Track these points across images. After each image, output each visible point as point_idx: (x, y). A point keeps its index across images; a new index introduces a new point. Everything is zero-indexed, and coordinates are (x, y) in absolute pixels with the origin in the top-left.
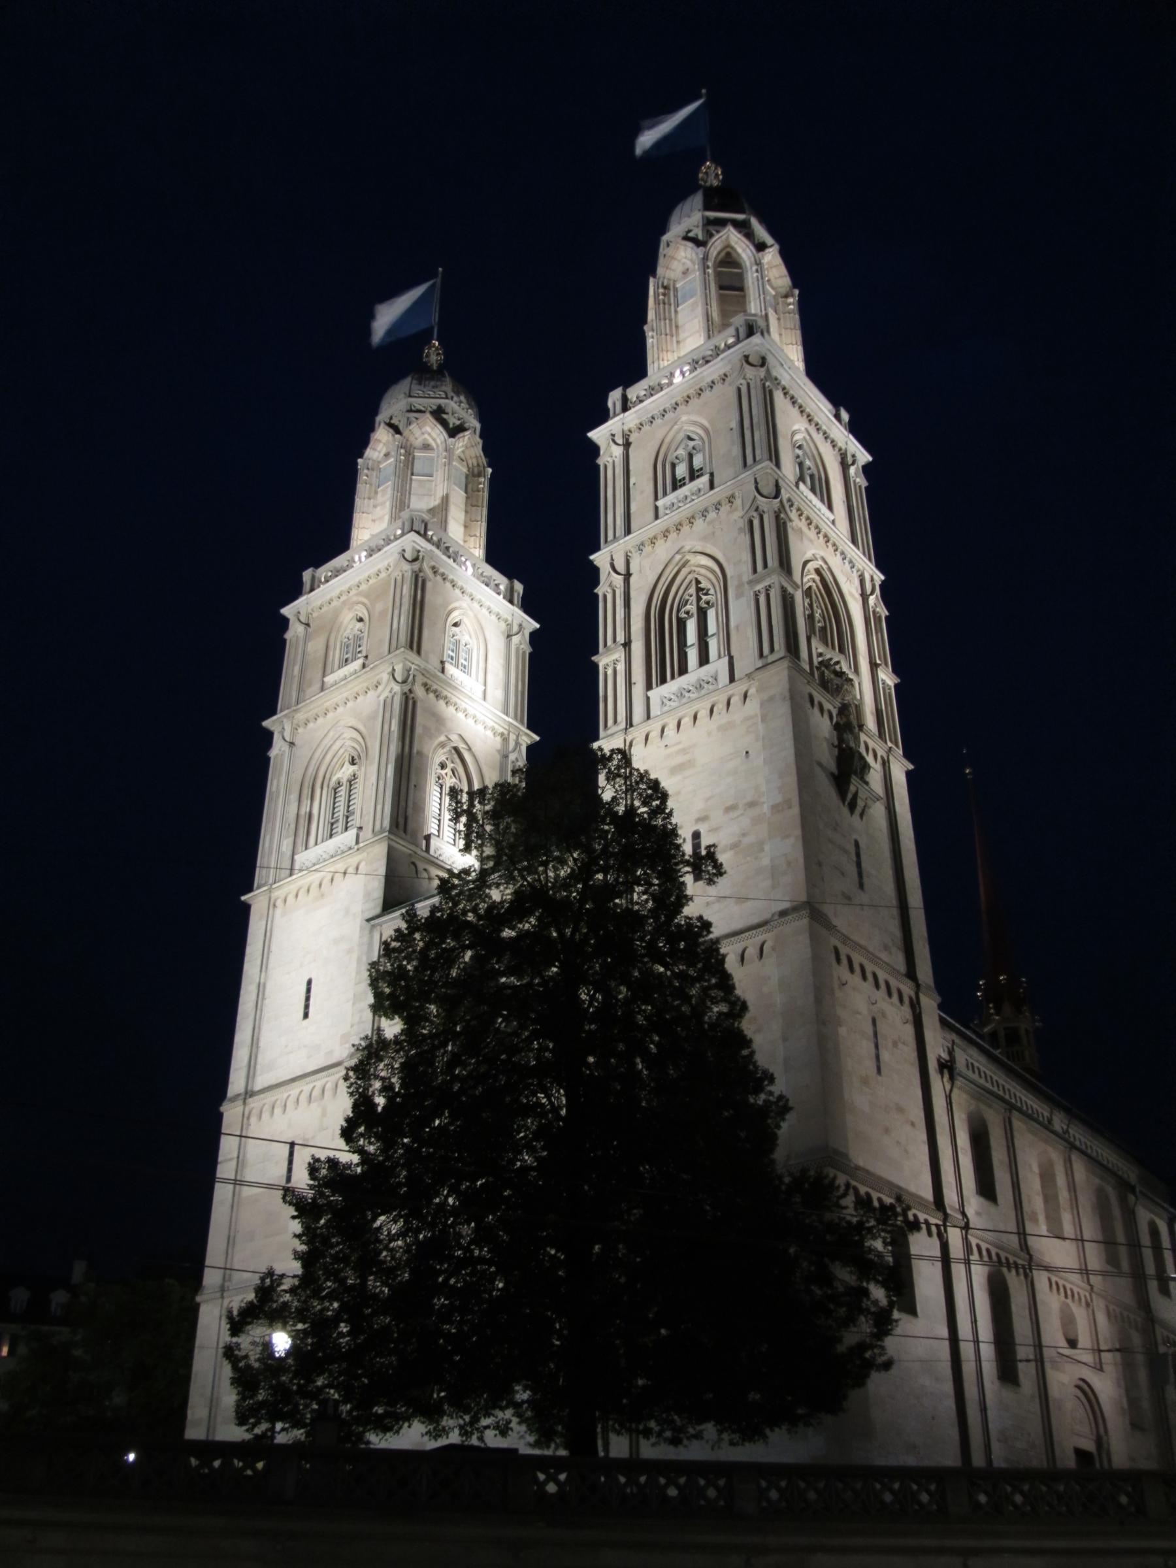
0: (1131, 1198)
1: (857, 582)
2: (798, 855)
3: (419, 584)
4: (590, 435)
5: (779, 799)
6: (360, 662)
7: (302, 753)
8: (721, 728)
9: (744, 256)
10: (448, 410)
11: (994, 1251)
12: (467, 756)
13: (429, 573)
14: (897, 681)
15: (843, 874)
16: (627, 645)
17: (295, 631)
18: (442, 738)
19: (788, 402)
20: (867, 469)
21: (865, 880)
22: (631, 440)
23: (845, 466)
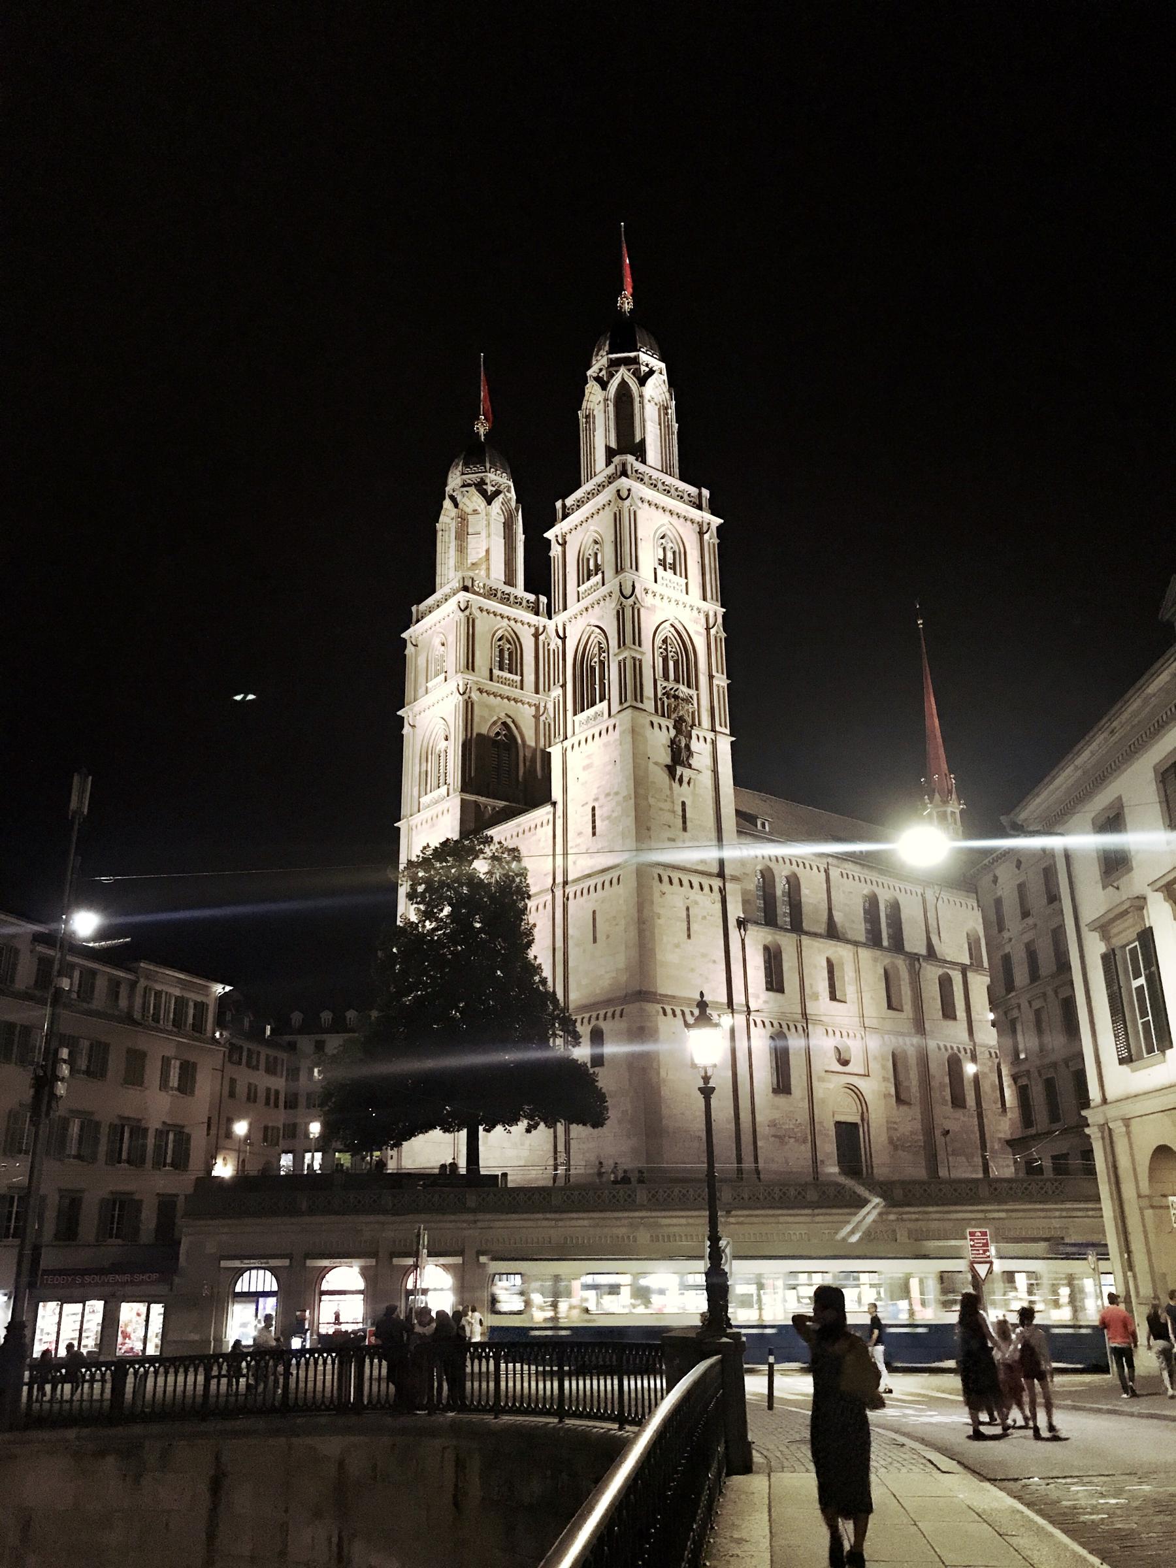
1: (703, 621)
3: (471, 623)
4: (545, 535)
5: (625, 794)
6: (443, 675)
7: (418, 731)
8: (606, 745)
10: (488, 481)
12: (512, 725)
13: (477, 613)
16: (564, 686)
17: (410, 650)
18: (495, 718)
19: (653, 507)
21: (688, 824)
22: (567, 539)
23: (701, 534)
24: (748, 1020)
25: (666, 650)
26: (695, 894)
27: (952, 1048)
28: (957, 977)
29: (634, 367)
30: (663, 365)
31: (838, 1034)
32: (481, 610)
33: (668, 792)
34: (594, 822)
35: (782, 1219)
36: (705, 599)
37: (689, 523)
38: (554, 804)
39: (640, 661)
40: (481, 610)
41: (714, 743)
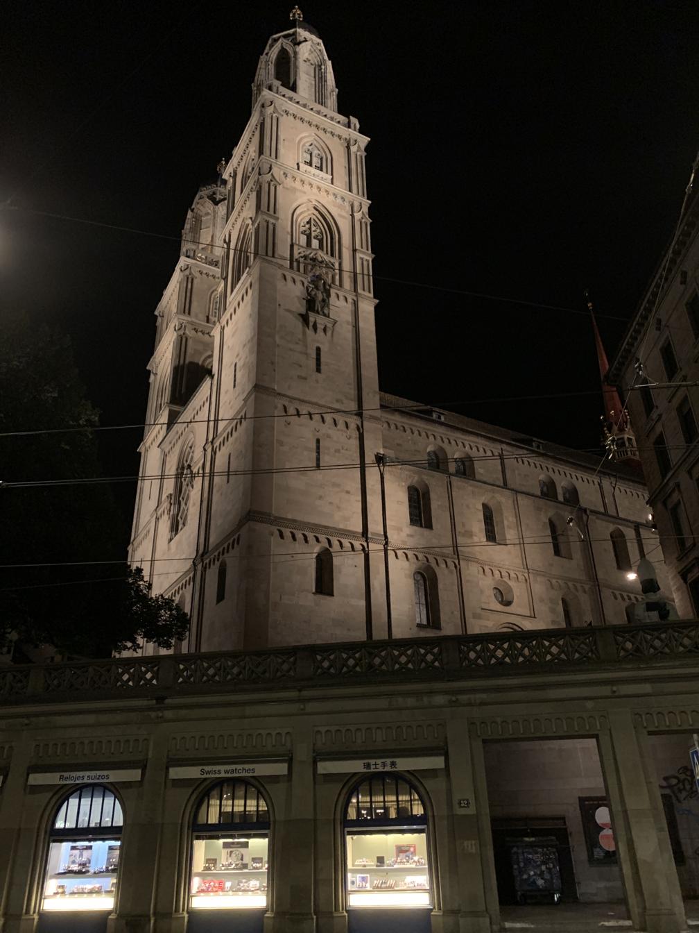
0: (585, 518)
1: (349, 209)
2: (255, 362)
8: (246, 306)
9: (290, 52)
11: (421, 556)
14: (374, 256)
15: (301, 366)
17: (159, 319)
19: (298, 121)
20: (368, 148)
21: (323, 367)
23: (348, 148)
24: (386, 551)
25: (310, 228)
26: (327, 429)
27: (630, 599)
28: (630, 533)
29: (291, 38)
30: (321, 41)
31: (497, 573)
32: (201, 273)
33: (300, 336)
34: (235, 376)
35: (249, 710)
36: (350, 190)
37: (336, 139)
38: (212, 377)
39: (274, 225)
40: (201, 273)
41: (355, 304)
